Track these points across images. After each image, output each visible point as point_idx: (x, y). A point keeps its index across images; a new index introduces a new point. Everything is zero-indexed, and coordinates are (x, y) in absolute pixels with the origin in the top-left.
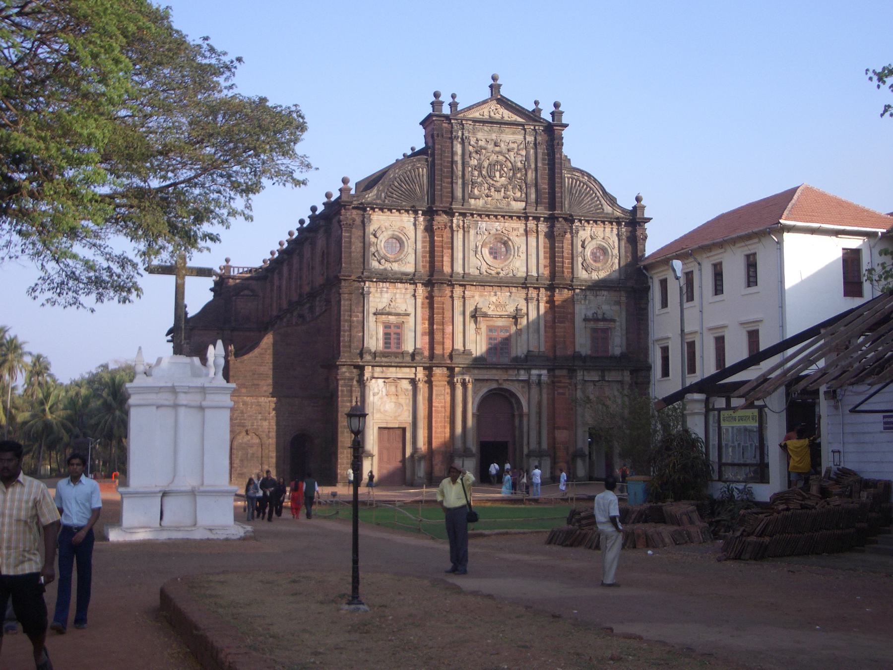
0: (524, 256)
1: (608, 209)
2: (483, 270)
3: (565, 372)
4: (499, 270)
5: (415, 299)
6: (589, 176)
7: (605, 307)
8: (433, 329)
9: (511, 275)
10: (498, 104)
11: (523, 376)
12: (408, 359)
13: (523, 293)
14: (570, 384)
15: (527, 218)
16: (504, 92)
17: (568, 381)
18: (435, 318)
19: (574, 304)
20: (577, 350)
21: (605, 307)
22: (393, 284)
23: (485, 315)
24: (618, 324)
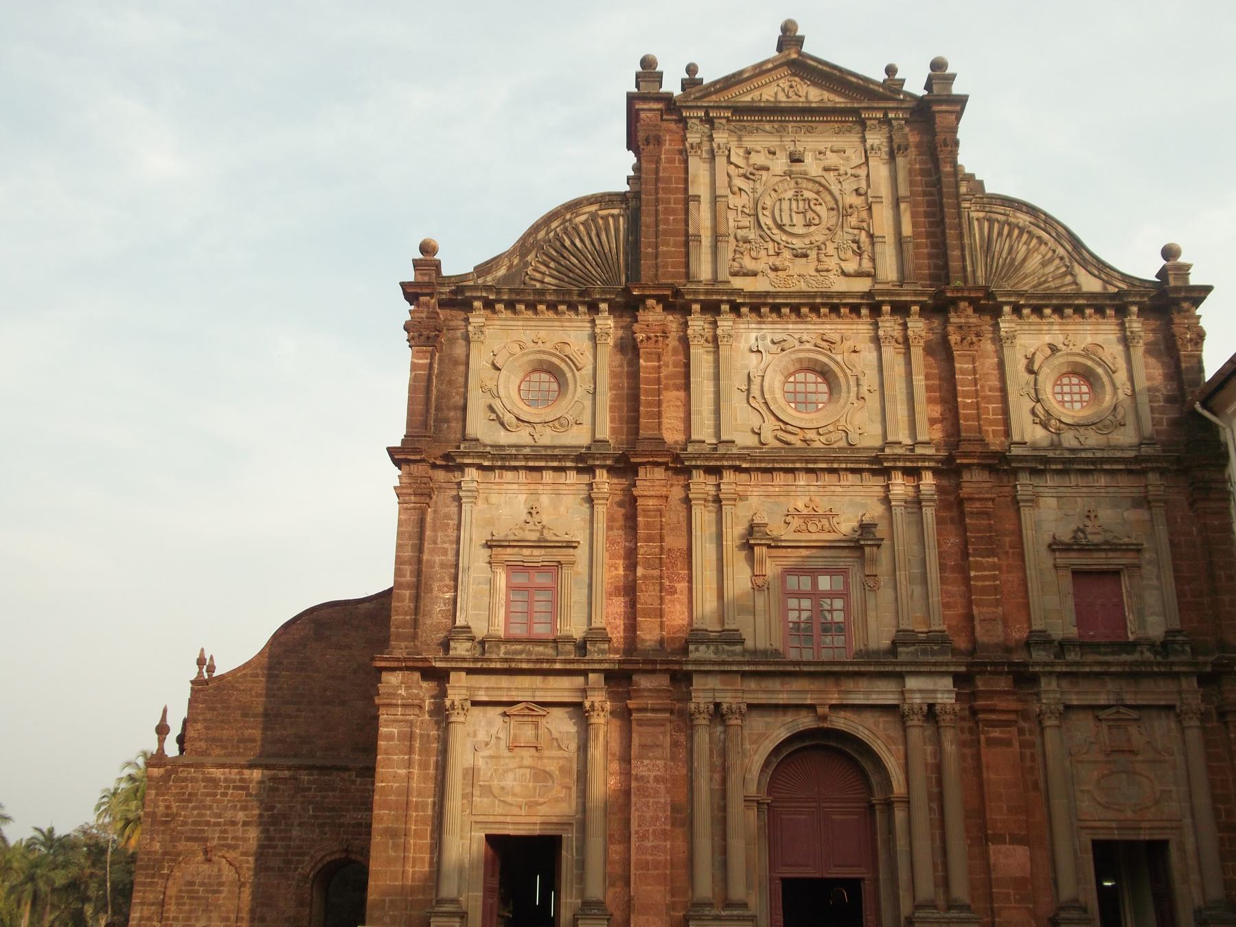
0: (873, 402)
1: (1090, 284)
2: (768, 436)
3: (1003, 684)
4: (811, 435)
5: (592, 507)
6: (1032, 210)
7: (1106, 515)
8: (635, 580)
9: (843, 444)
10: (794, 75)
11: (885, 693)
12: (569, 651)
13: (875, 485)
14: (1025, 715)
15: (875, 310)
16: (807, 48)
17: (1012, 704)
18: (641, 551)
19: (1018, 509)
20: (1037, 625)
21: (1106, 515)
22: (536, 475)
23: (774, 545)
24: (1147, 555)
